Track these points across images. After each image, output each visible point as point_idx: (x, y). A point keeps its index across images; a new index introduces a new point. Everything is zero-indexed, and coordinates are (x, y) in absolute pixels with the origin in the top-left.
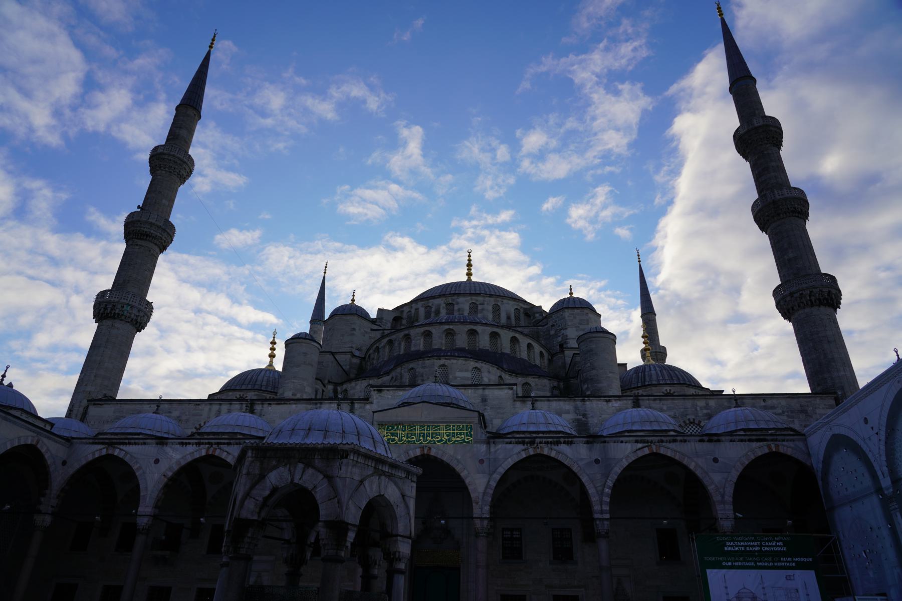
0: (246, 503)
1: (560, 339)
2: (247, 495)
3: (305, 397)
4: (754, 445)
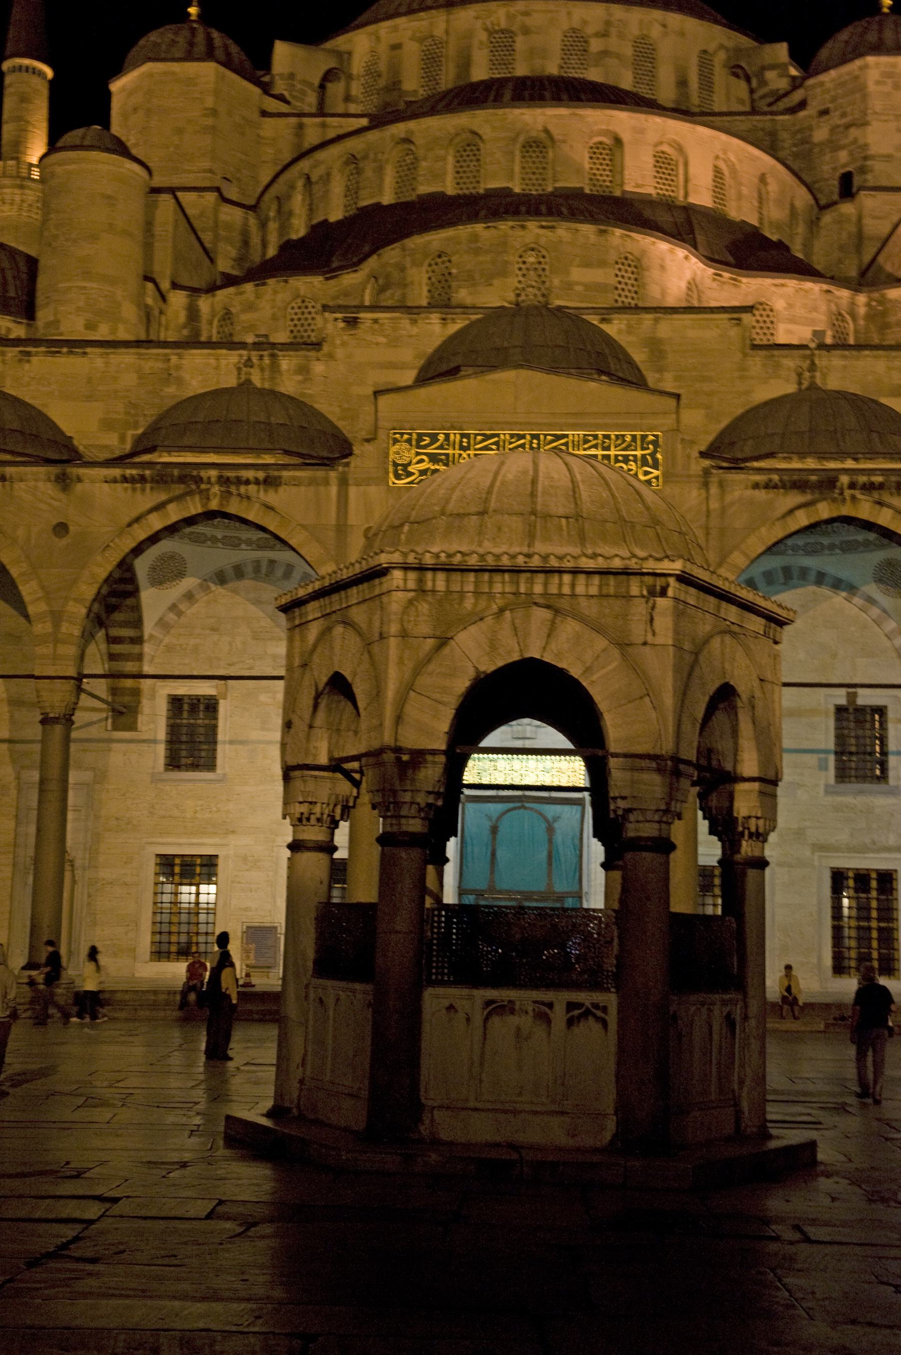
2: (408, 688)
3: (123, 335)
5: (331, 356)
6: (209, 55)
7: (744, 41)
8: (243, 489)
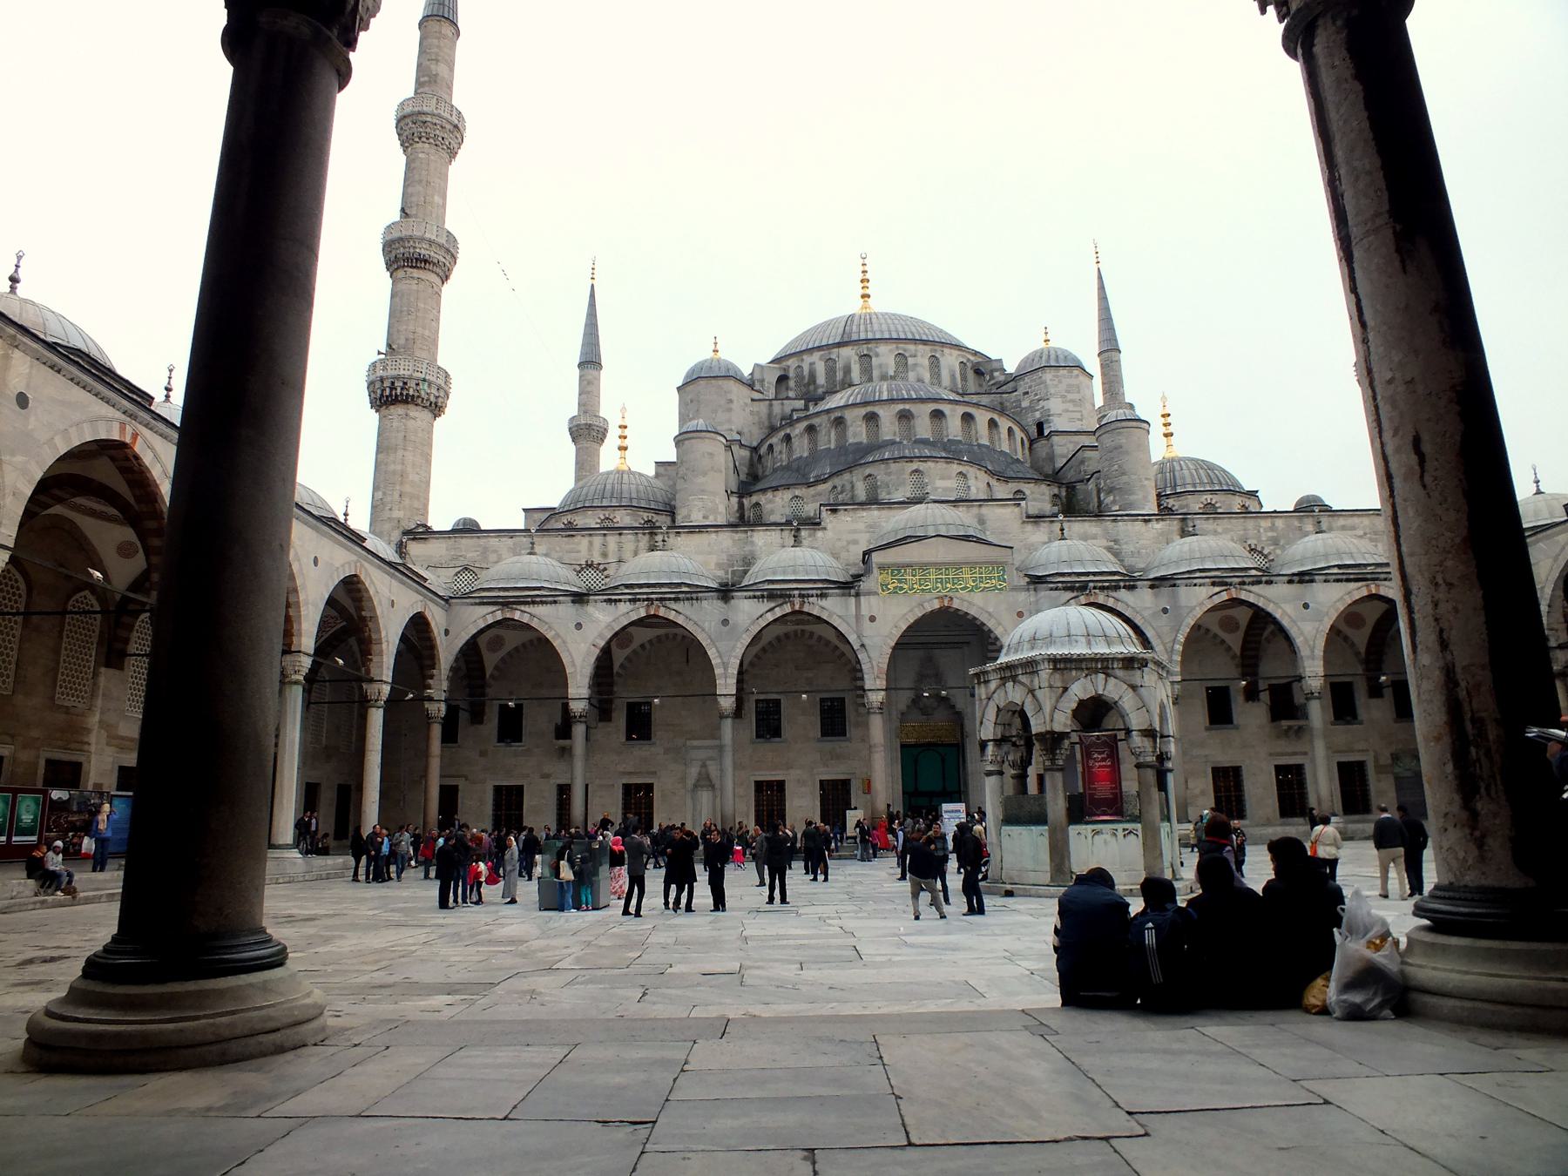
1: (1038, 415)
3: (721, 521)
4: (1353, 585)
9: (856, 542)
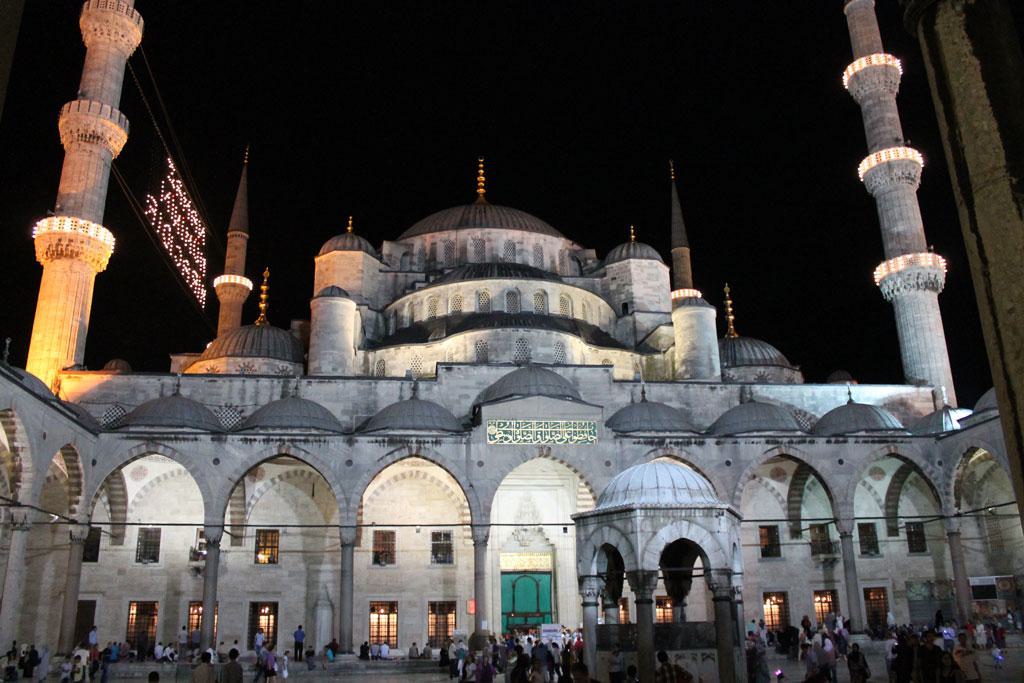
0: (646, 556)
1: (623, 296)
2: (645, 550)
4: (877, 446)
5: (440, 383)
6: (360, 248)
7: (576, 247)
8: (427, 445)
9: (468, 397)
